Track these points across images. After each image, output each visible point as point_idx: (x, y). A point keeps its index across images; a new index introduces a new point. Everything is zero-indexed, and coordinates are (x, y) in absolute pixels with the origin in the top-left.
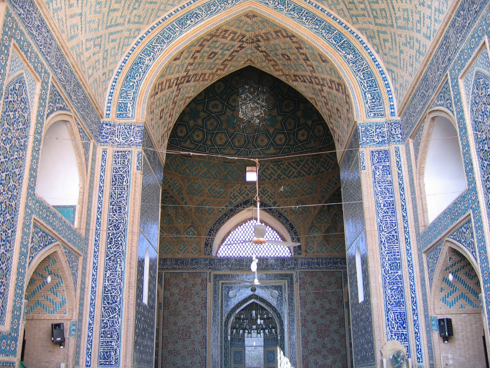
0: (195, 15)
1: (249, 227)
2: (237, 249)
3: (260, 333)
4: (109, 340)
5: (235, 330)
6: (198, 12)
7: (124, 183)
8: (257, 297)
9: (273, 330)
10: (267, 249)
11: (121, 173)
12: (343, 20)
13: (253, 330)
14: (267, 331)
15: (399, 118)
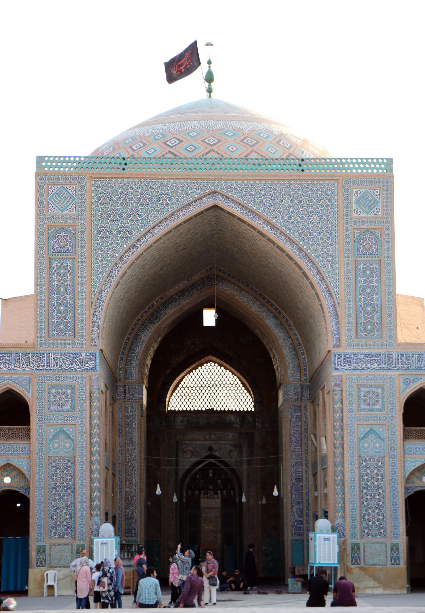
0: (174, 300)
1: (205, 371)
2: (192, 397)
3: (217, 494)
4: (131, 522)
5: (190, 491)
6: (176, 297)
7: (134, 426)
8: (214, 457)
9: (232, 491)
10: (226, 397)
11: (131, 419)
12: (277, 307)
13: (210, 490)
14: (225, 492)
15: (309, 384)
